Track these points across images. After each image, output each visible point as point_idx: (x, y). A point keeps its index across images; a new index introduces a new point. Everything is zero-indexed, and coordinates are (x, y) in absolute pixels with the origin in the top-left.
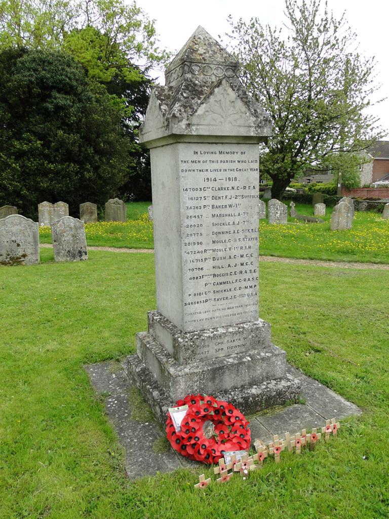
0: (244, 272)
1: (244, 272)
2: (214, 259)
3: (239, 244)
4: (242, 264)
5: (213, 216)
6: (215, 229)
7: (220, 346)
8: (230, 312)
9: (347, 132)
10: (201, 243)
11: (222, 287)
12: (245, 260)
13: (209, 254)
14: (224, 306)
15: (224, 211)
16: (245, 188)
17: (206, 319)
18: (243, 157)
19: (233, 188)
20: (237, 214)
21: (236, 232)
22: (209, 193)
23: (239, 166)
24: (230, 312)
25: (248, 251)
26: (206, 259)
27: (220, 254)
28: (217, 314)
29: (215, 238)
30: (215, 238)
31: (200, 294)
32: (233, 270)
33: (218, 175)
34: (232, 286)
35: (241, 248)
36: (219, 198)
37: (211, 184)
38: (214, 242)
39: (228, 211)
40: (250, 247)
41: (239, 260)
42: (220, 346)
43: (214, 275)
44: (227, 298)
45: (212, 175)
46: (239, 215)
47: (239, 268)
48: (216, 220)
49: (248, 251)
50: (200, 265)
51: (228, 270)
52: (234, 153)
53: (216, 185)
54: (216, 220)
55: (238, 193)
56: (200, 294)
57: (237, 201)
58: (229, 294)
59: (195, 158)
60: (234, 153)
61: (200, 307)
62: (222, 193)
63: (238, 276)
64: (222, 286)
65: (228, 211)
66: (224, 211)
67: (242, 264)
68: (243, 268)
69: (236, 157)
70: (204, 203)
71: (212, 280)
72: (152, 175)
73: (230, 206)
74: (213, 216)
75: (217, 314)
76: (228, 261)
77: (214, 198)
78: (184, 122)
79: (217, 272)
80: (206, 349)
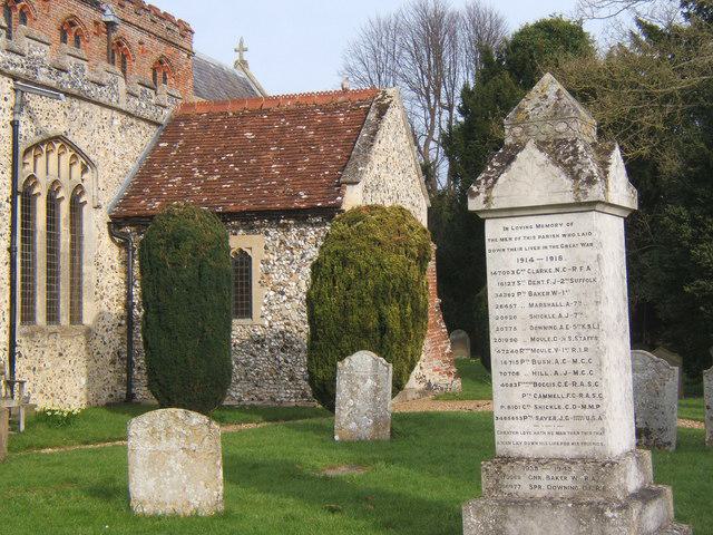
0: (579, 384)
1: (579, 384)
2: (534, 362)
3: (567, 344)
4: (576, 373)
5: (531, 305)
6: (535, 323)
7: (537, 482)
8: (560, 439)
9: (693, 119)
10: (515, 340)
11: (547, 402)
12: (580, 367)
13: (527, 355)
14: (551, 429)
15: (543, 300)
16: (574, 269)
17: (525, 443)
18: (571, 230)
19: (557, 270)
20: (564, 303)
21: (564, 327)
22: (524, 277)
23: (566, 241)
24: (560, 439)
25: (585, 356)
26: (522, 361)
27: (542, 356)
28: (541, 438)
29: (533, 334)
30: (533, 334)
31: (516, 407)
32: (562, 379)
33: (536, 254)
34: (563, 403)
35: (574, 349)
36: (539, 282)
37: (526, 266)
38: (532, 339)
39: (551, 299)
40: (586, 350)
41: (570, 367)
42: (537, 482)
43: (535, 384)
44: (555, 418)
45: (527, 255)
46: (568, 304)
47: (570, 378)
48: (534, 311)
49: (585, 356)
50: (515, 368)
51: (555, 379)
52: (556, 225)
53: (534, 266)
54: (534, 311)
55: (564, 275)
56: (516, 407)
57: (564, 287)
58: (558, 413)
59: (504, 235)
60: (556, 225)
61: (518, 425)
62: (541, 277)
63: (570, 389)
64: (547, 400)
65: (551, 299)
66: (543, 300)
67: (576, 373)
68: (579, 379)
69: (560, 230)
70: (519, 289)
71: (530, 389)
72: (493, 285)
73: (554, 293)
74: (531, 305)
75: (541, 438)
76: (553, 367)
77: (530, 282)
78: (482, 197)
79: (539, 380)
80: (516, 482)
